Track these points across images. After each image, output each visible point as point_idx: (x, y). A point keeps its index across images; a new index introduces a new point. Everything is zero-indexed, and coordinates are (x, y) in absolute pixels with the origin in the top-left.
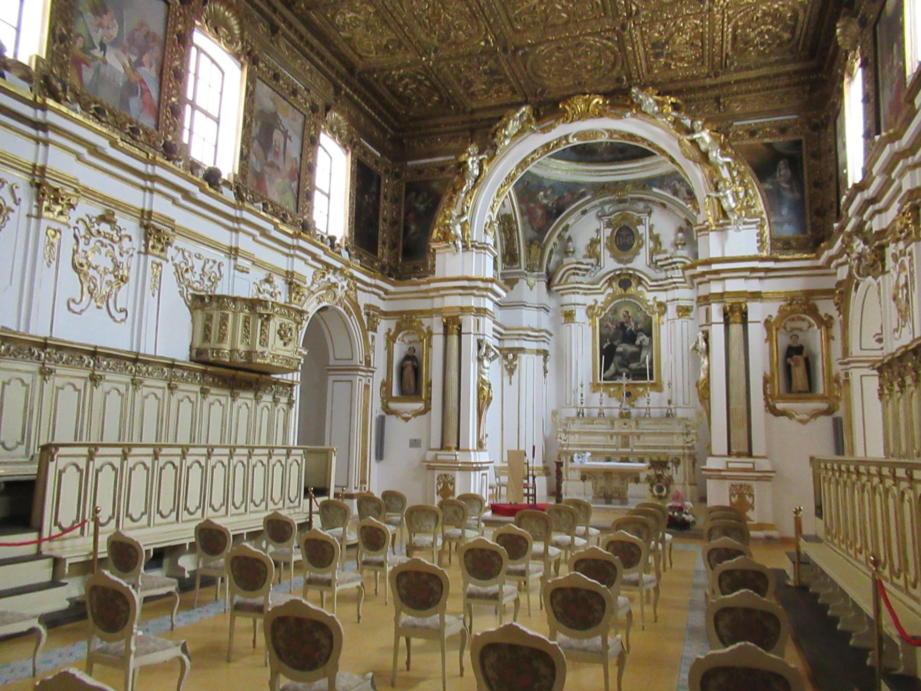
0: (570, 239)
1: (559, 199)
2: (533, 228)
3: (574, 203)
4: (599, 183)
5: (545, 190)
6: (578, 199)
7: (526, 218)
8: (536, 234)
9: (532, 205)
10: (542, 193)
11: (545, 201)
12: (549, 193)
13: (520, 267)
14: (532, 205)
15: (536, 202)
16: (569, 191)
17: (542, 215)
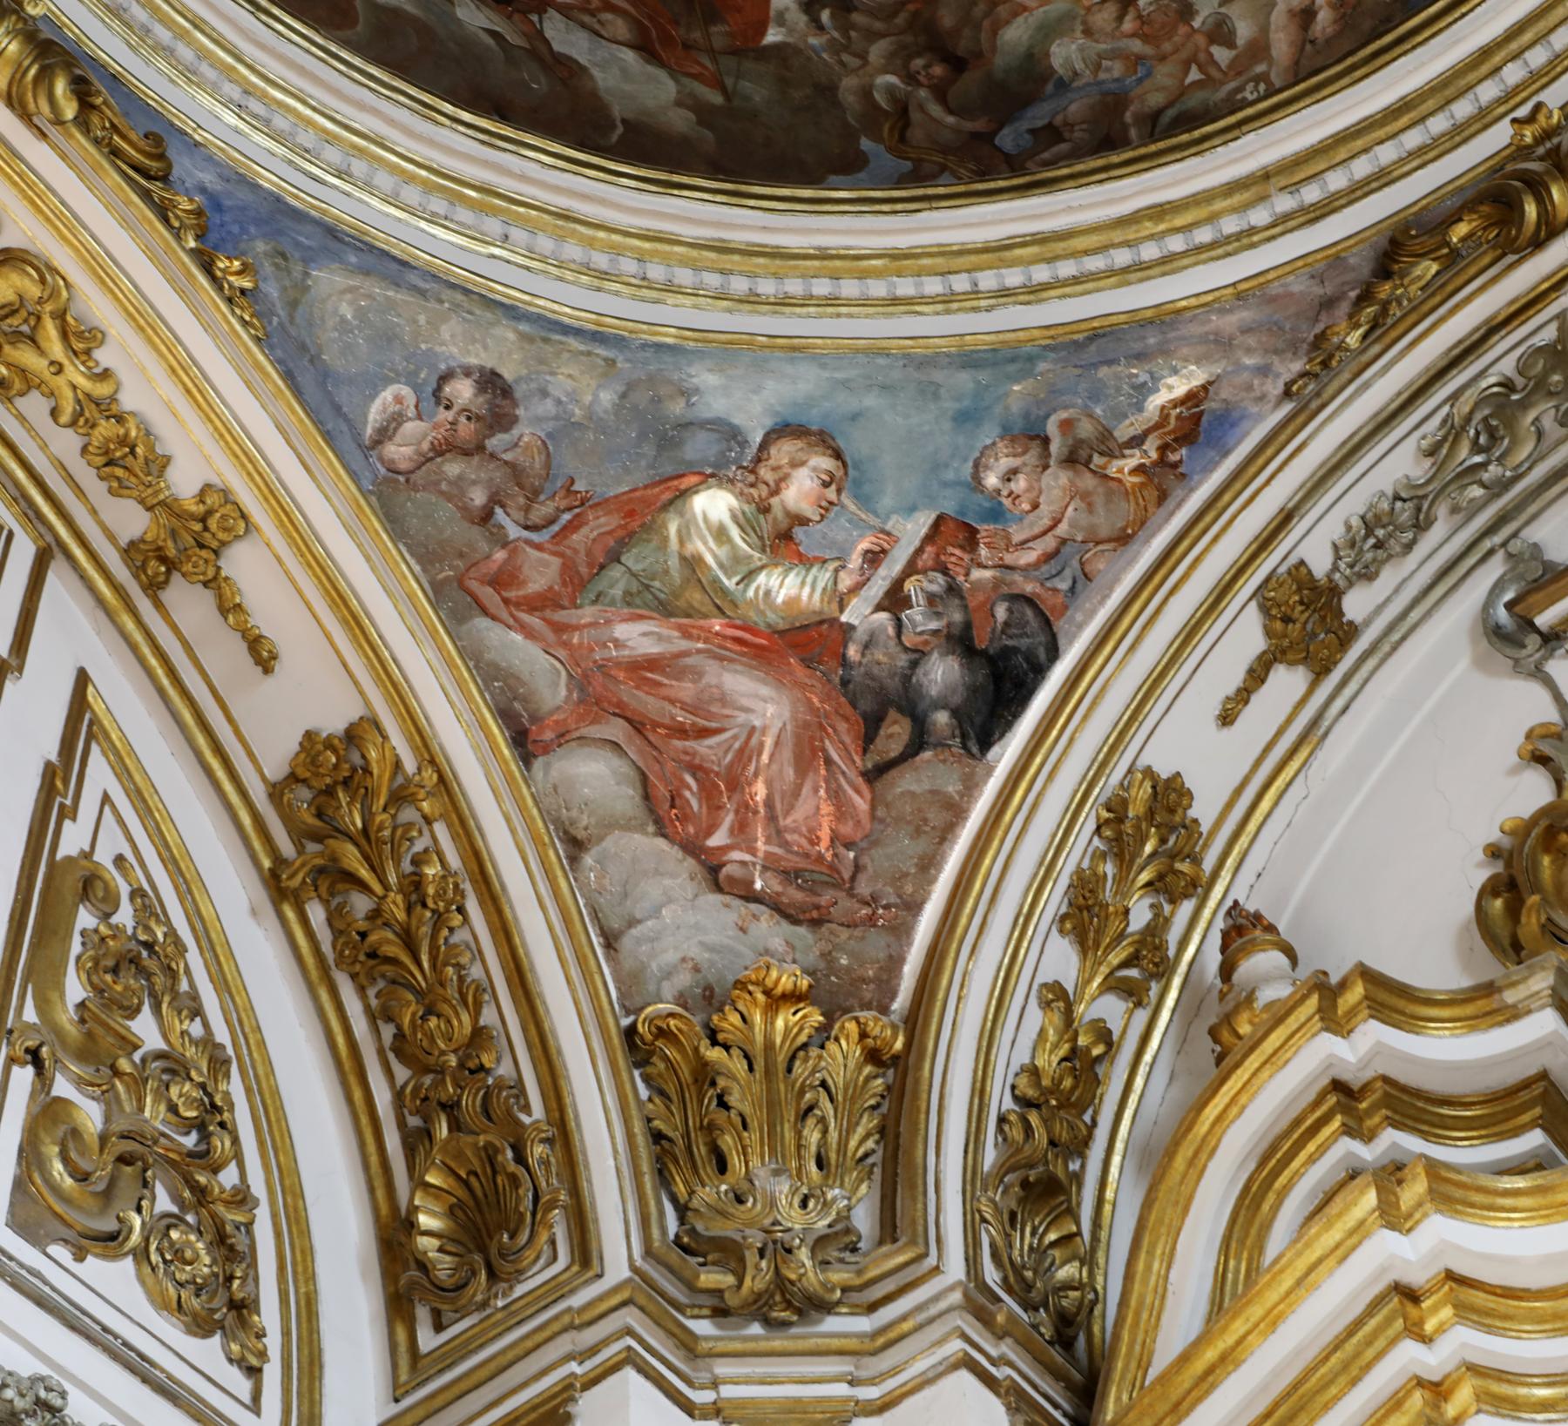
0: (1243, 930)
1: (955, 533)
2: (714, 875)
3: (1123, 539)
4: (1333, 258)
5: (742, 461)
6: (1163, 479)
7: (594, 775)
8: (770, 931)
9: (638, 637)
10: (714, 504)
11: (786, 589)
12: (800, 489)
13: (585, 1254)
14: (638, 637)
15: (682, 597)
16: (1032, 436)
17: (807, 751)
